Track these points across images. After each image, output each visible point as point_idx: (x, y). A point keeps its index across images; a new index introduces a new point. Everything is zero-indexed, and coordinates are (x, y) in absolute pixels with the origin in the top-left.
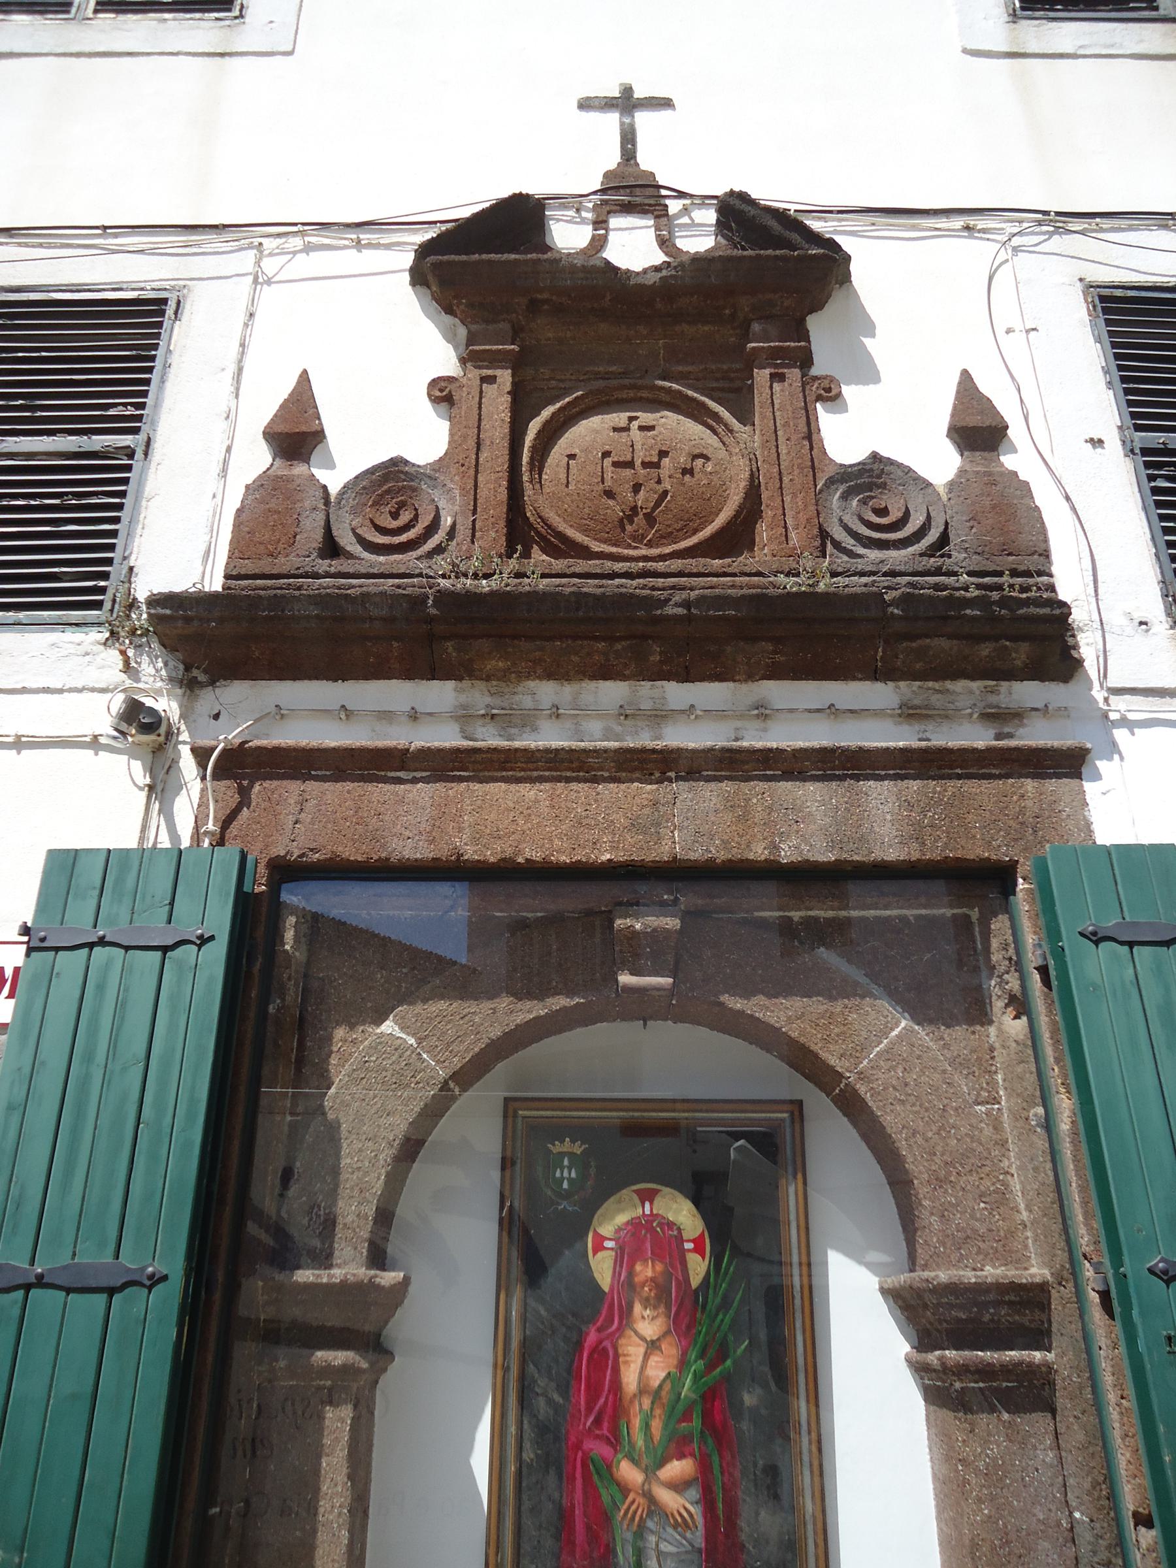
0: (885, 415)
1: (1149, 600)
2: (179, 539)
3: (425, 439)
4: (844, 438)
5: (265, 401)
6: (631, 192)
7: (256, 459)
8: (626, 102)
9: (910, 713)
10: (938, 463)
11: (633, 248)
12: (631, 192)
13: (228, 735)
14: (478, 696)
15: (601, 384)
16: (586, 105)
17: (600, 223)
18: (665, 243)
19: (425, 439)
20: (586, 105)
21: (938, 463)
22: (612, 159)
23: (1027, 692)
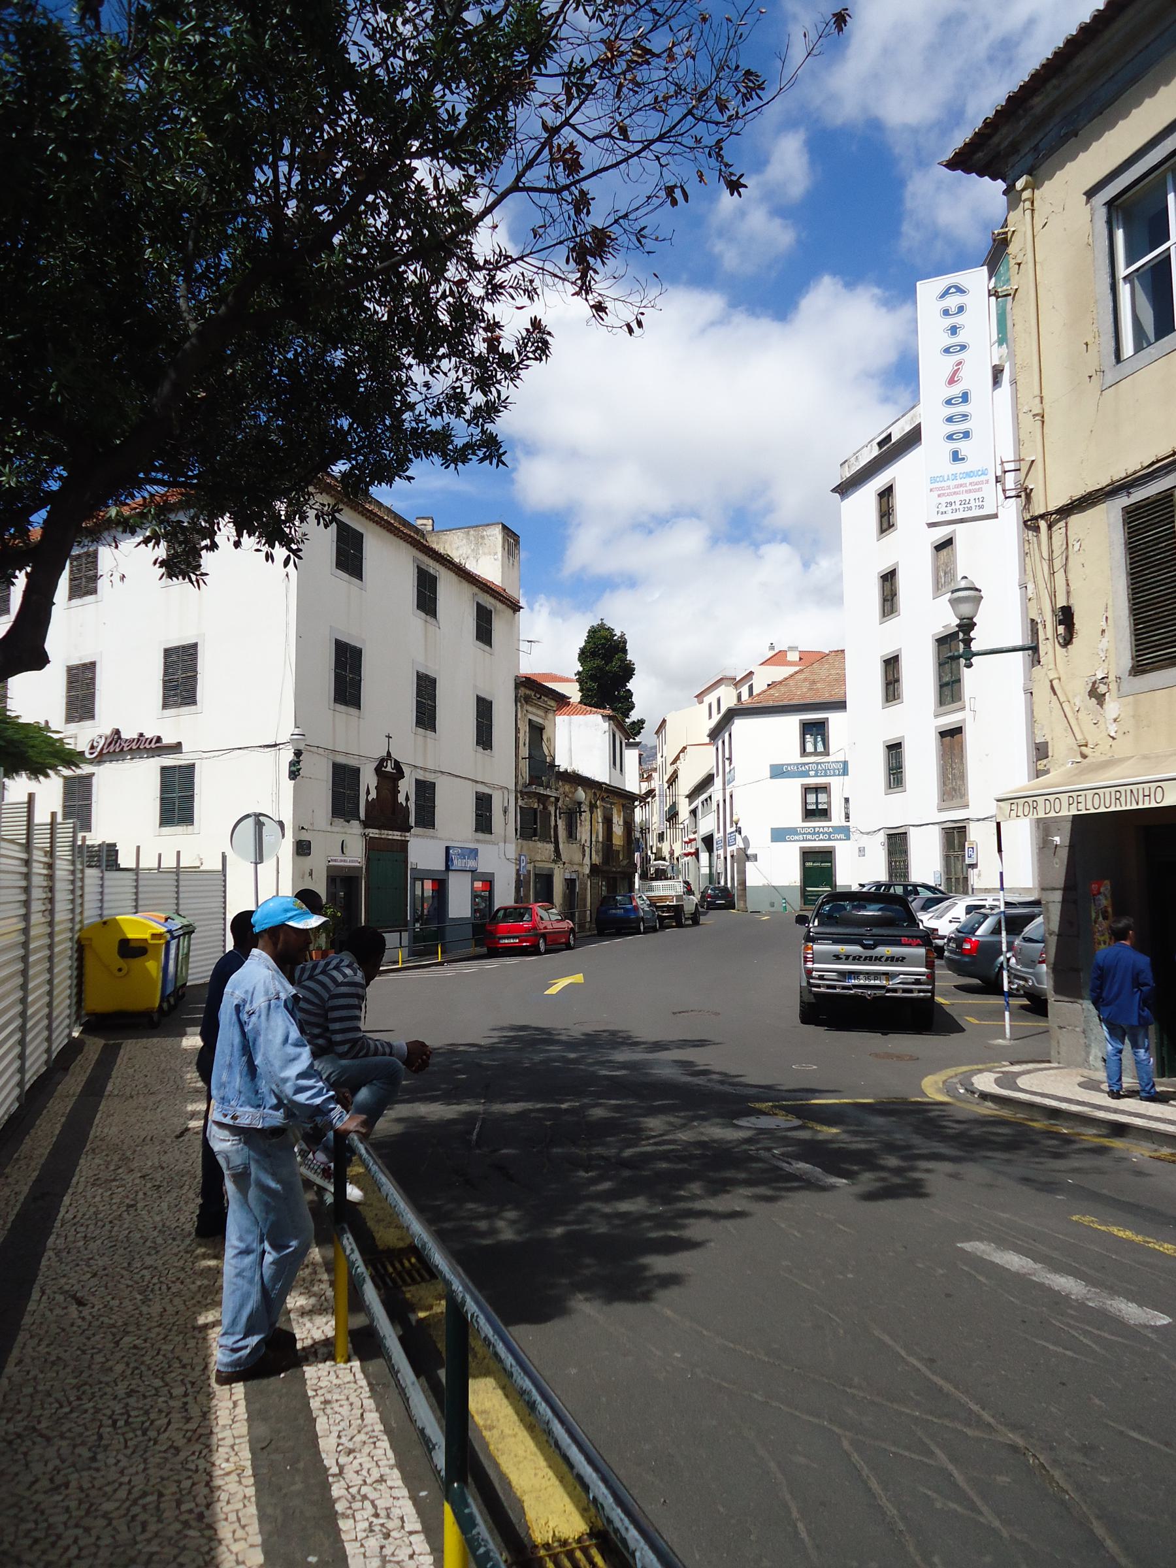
8: (389, 737)
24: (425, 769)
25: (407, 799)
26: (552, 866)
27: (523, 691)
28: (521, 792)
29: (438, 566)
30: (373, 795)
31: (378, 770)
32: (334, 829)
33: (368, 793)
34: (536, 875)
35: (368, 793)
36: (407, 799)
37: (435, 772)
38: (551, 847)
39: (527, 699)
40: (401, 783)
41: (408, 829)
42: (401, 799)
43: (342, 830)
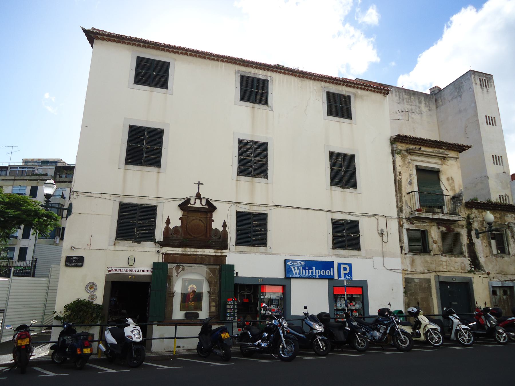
0: (217, 225)
1: (234, 244)
2: (159, 235)
3: (179, 223)
4: (214, 226)
5: (165, 220)
6: (198, 196)
7: (165, 225)
8: (199, 184)
9: (215, 252)
10: (221, 229)
11: (198, 204)
12: (198, 196)
13: (164, 252)
14: (183, 249)
15: (194, 218)
16: (195, 183)
17: (195, 201)
18: (201, 204)
19: (179, 223)
20: (195, 183)
21: (221, 229)
22: (197, 192)
23: (224, 251)
24: (252, 205)
25: (225, 225)
26: (470, 275)
27: (400, 146)
28: (408, 219)
29: (269, 73)
30: (176, 223)
31: (185, 206)
32: (117, 248)
33: (168, 222)
34: (443, 285)
35: (168, 222)
36: (225, 225)
37: (267, 206)
38: (466, 261)
39: (410, 152)
40: (215, 216)
41: (226, 247)
42: (217, 225)
43: (129, 249)
